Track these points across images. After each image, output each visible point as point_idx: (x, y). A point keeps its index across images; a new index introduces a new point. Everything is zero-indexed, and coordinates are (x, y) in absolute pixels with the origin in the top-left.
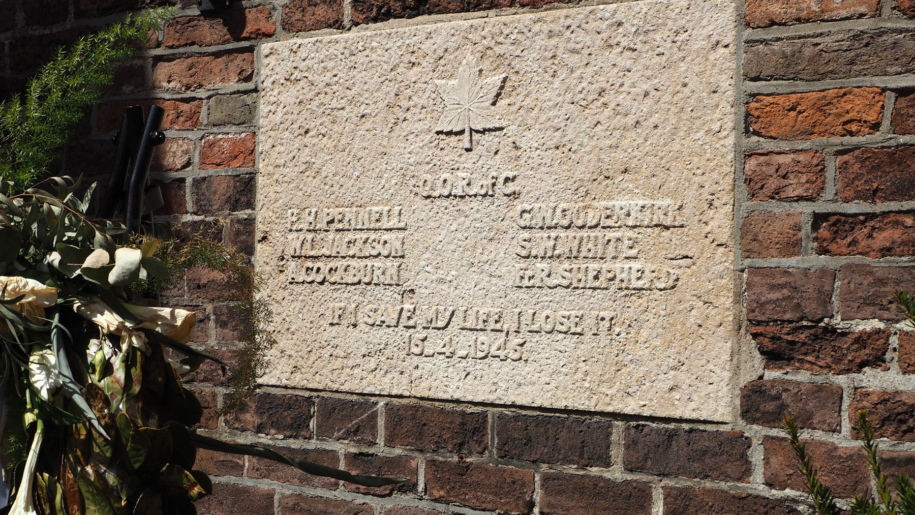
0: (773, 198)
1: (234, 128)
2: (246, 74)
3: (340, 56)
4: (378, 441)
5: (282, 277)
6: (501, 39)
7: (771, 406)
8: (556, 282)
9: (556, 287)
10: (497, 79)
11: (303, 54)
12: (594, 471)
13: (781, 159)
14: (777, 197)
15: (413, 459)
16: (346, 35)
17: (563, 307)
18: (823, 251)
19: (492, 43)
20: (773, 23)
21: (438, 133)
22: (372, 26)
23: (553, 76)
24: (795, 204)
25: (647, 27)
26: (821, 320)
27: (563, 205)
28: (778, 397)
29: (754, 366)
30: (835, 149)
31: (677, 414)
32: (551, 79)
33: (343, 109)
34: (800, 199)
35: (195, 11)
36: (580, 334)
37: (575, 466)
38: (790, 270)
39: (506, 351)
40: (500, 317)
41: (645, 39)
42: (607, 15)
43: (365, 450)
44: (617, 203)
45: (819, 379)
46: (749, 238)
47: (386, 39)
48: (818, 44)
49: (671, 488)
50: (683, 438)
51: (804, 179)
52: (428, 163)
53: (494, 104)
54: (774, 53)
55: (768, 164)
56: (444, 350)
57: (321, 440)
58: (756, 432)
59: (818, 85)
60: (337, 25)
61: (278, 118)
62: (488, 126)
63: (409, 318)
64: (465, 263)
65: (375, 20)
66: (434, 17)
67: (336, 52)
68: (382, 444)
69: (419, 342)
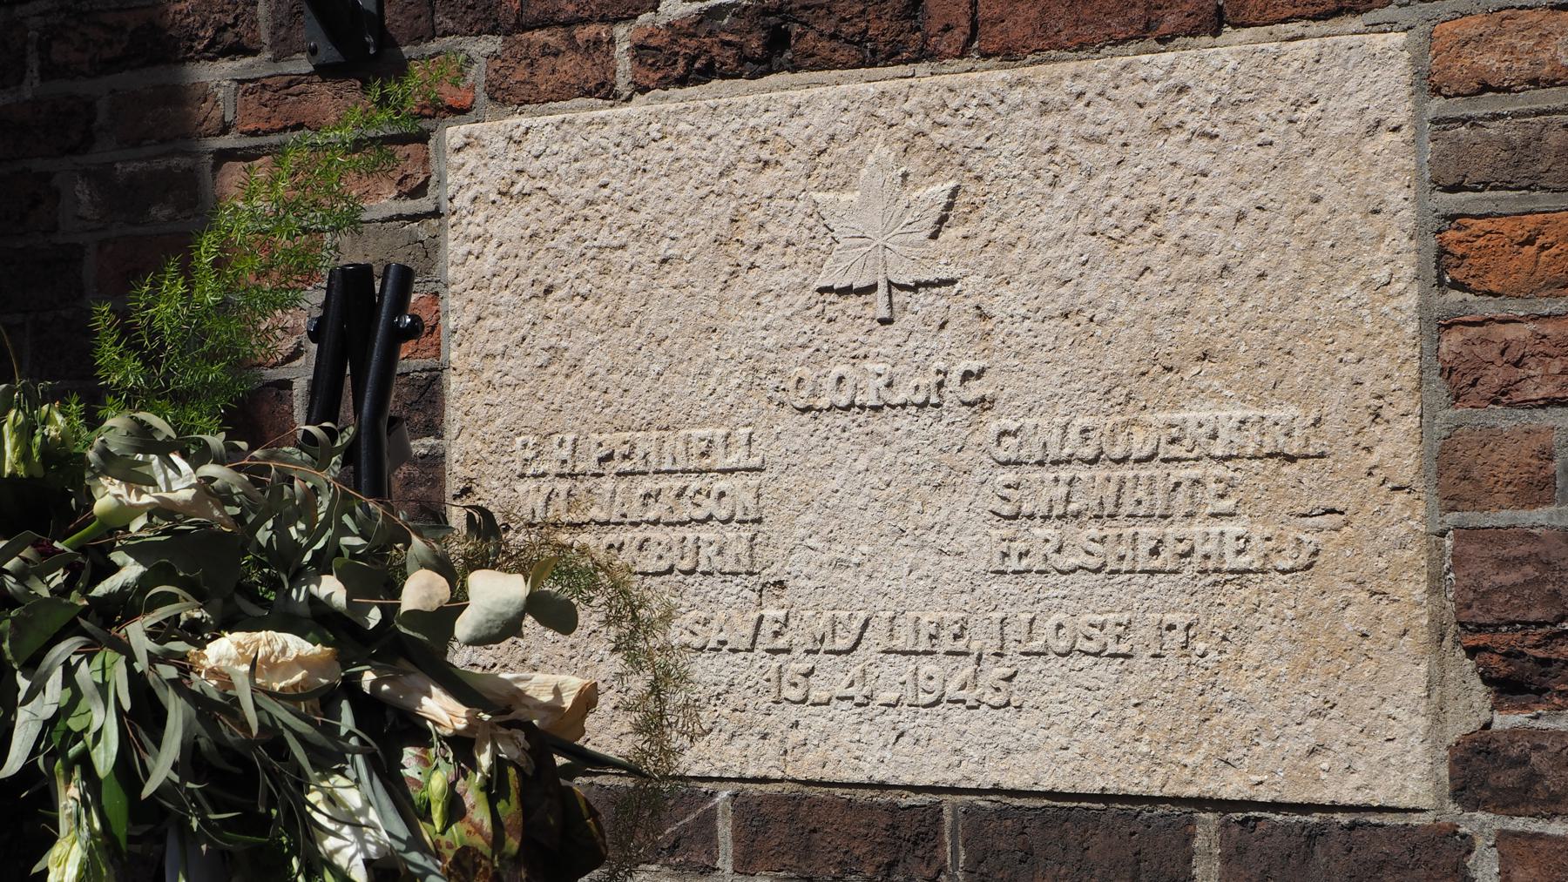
0: (1496, 402)
2: (411, 184)
3: (613, 150)
4: (719, 864)
6: (944, 117)
7: (1509, 778)
8: (1073, 561)
9: (1074, 571)
10: (939, 190)
11: (534, 144)
13: (1510, 332)
16: (623, 111)
17: (1093, 608)
20: (1485, 87)
21: (822, 291)
22: (675, 92)
24: (1539, 413)
25: (1238, 95)
27: (1082, 421)
29: (1472, 707)
31: (1326, 797)
32: (1048, 190)
33: (623, 247)
34: (1550, 402)
35: (302, 65)
36: (1126, 656)
39: (978, 691)
40: (962, 628)
41: (1233, 117)
42: (1157, 73)
46: (1453, 475)
47: (707, 118)
52: (803, 347)
53: (934, 236)
54: (1489, 141)
55: (1485, 341)
56: (850, 692)
58: (1482, 824)
60: (605, 91)
61: (487, 265)
62: (924, 278)
63: (776, 634)
64: (887, 529)
65: (682, 82)
66: (803, 76)
67: (604, 142)
68: (729, 869)
69: (799, 679)
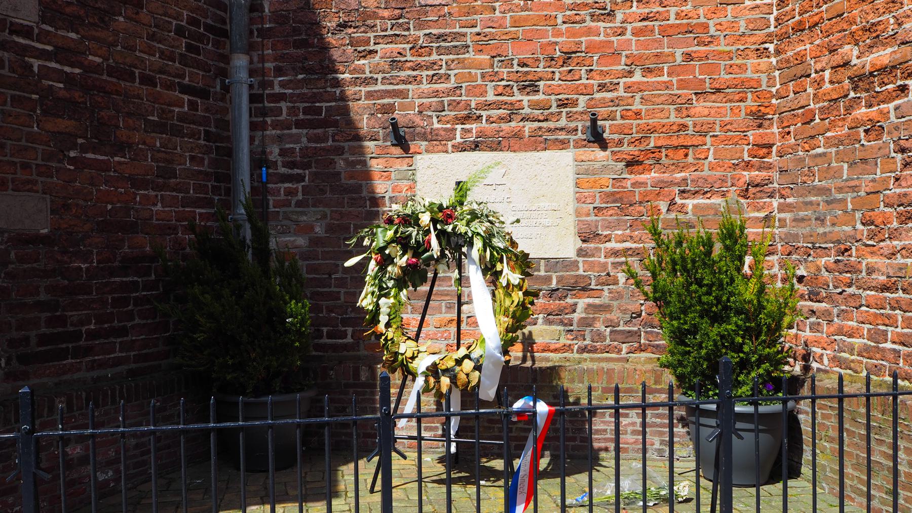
10: (504, 171)
29: (579, 244)
35: (389, 143)
46: (578, 213)
58: (581, 259)
60: (447, 152)
61: (425, 178)
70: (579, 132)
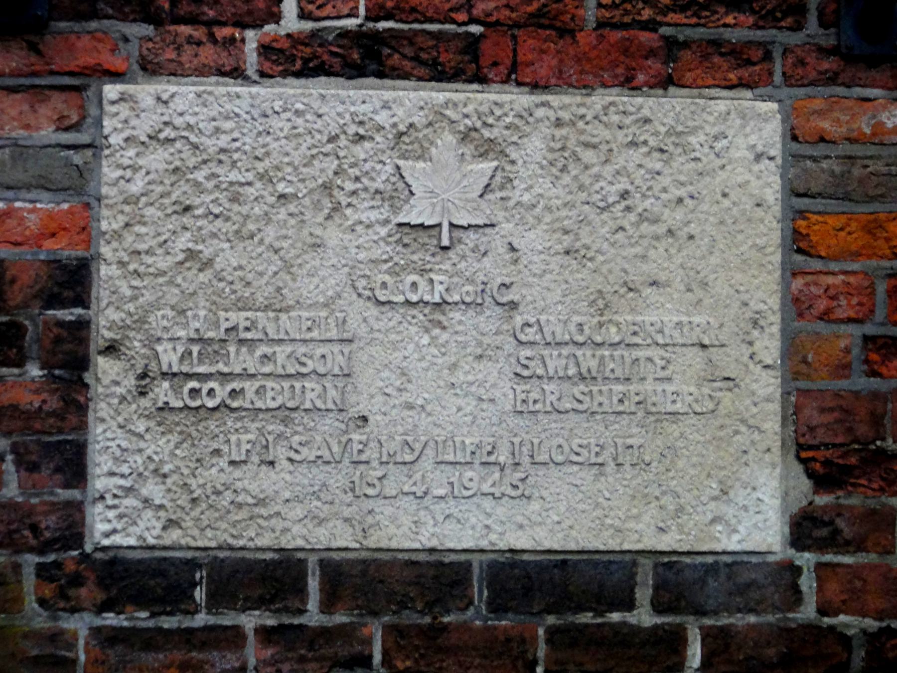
0: (821, 319)
1: (45, 195)
2: (67, 123)
3: (245, 116)
4: (309, 607)
5: (145, 402)
6: (490, 120)
7: (824, 532)
8: (568, 406)
9: (567, 412)
11: (179, 104)
12: (615, 617)
13: (830, 280)
14: (826, 317)
15: (365, 625)
16: (254, 89)
17: (587, 434)
18: (873, 373)
19: (478, 124)
20: (822, 140)
21: (400, 225)
22: (290, 80)
23: (562, 171)
25: (680, 128)
26: (873, 442)
27: (577, 319)
28: (831, 523)
30: (885, 272)
31: (719, 548)
32: (558, 174)
33: (249, 184)
36: (601, 465)
37: (591, 614)
38: (842, 393)
39: (503, 488)
40: (494, 447)
41: (677, 141)
42: (632, 109)
43: (287, 620)
44: (648, 318)
45: (872, 503)
47: (319, 101)
48: (867, 166)
49: (711, 627)
50: (723, 572)
51: (855, 301)
52: (386, 261)
53: (481, 196)
54: (823, 171)
55: (816, 284)
56: (414, 489)
57: (214, 614)
58: (806, 559)
59: (871, 208)
60: (236, 73)
62: (474, 222)
63: (360, 451)
64: (442, 383)
65: (298, 75)
66: (388, 82)
67: (237, 110)
68: (316, 610)
69: (376, 482)
70: (812, 19)
